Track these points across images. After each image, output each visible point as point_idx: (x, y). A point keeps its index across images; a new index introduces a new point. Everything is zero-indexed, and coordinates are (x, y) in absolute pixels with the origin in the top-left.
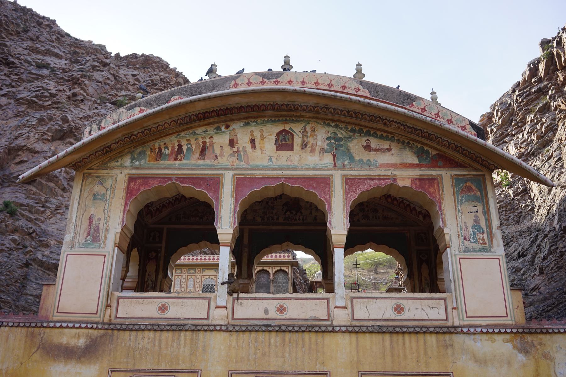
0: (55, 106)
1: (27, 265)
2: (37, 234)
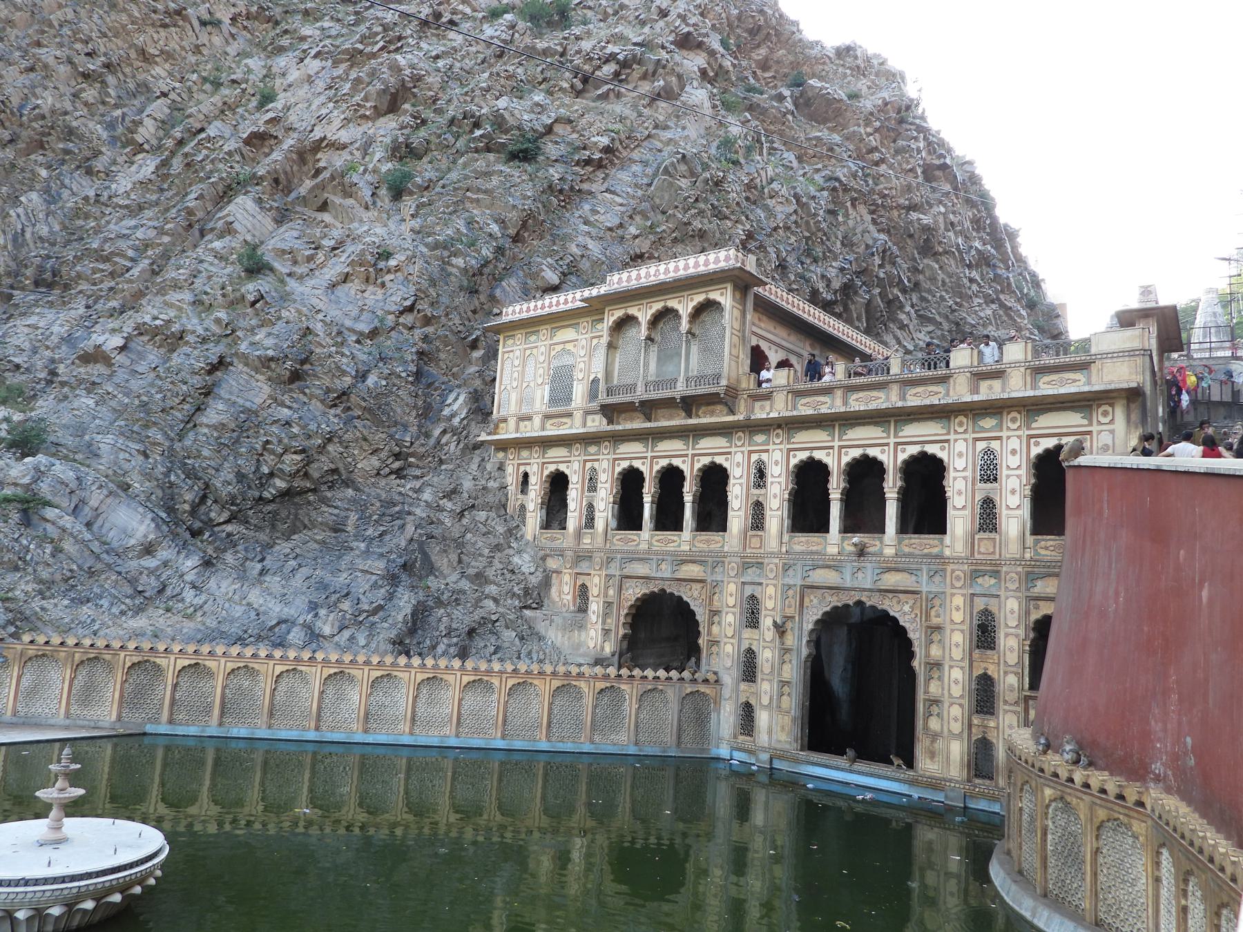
0: (392, 48)
1: (221, 364)
2: (267, 302)
